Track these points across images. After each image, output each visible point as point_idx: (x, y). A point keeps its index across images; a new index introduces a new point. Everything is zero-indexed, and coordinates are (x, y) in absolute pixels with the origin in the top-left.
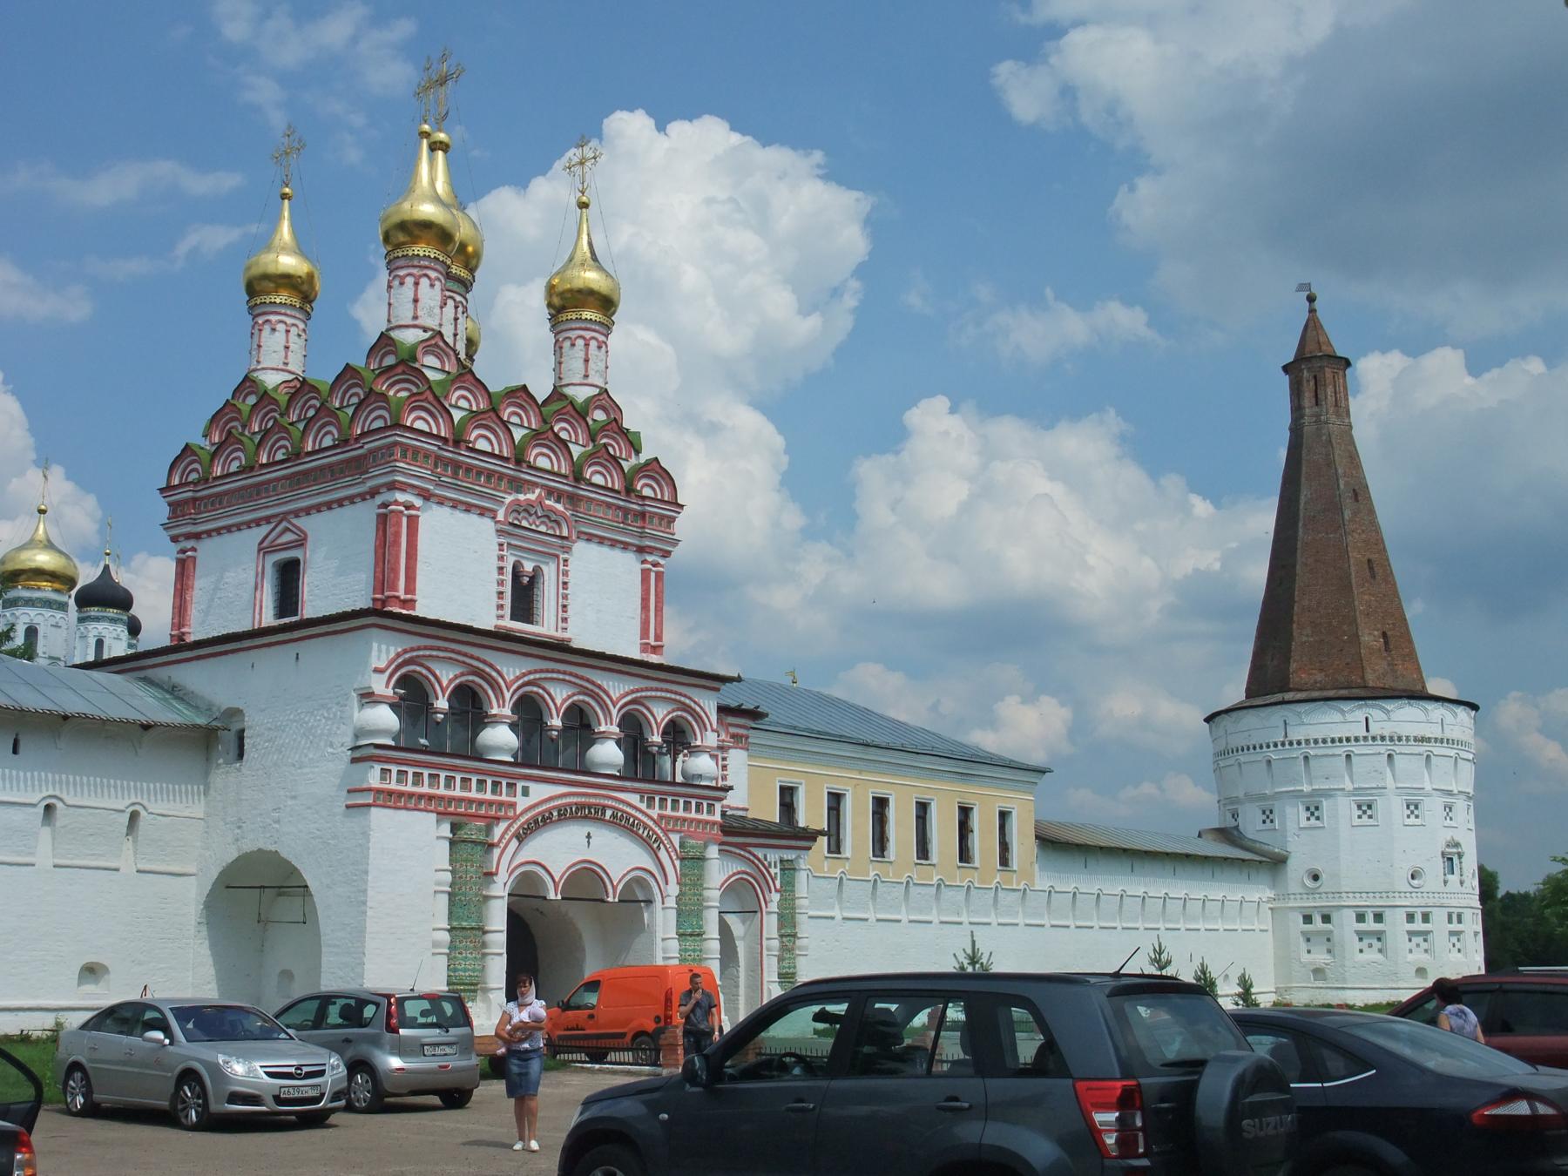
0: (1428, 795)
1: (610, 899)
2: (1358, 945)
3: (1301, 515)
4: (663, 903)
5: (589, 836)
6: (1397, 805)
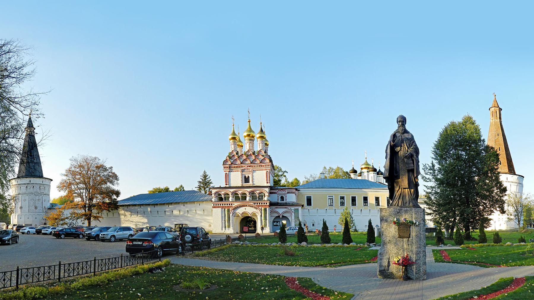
1: (250, 216)
5: (245, 209)
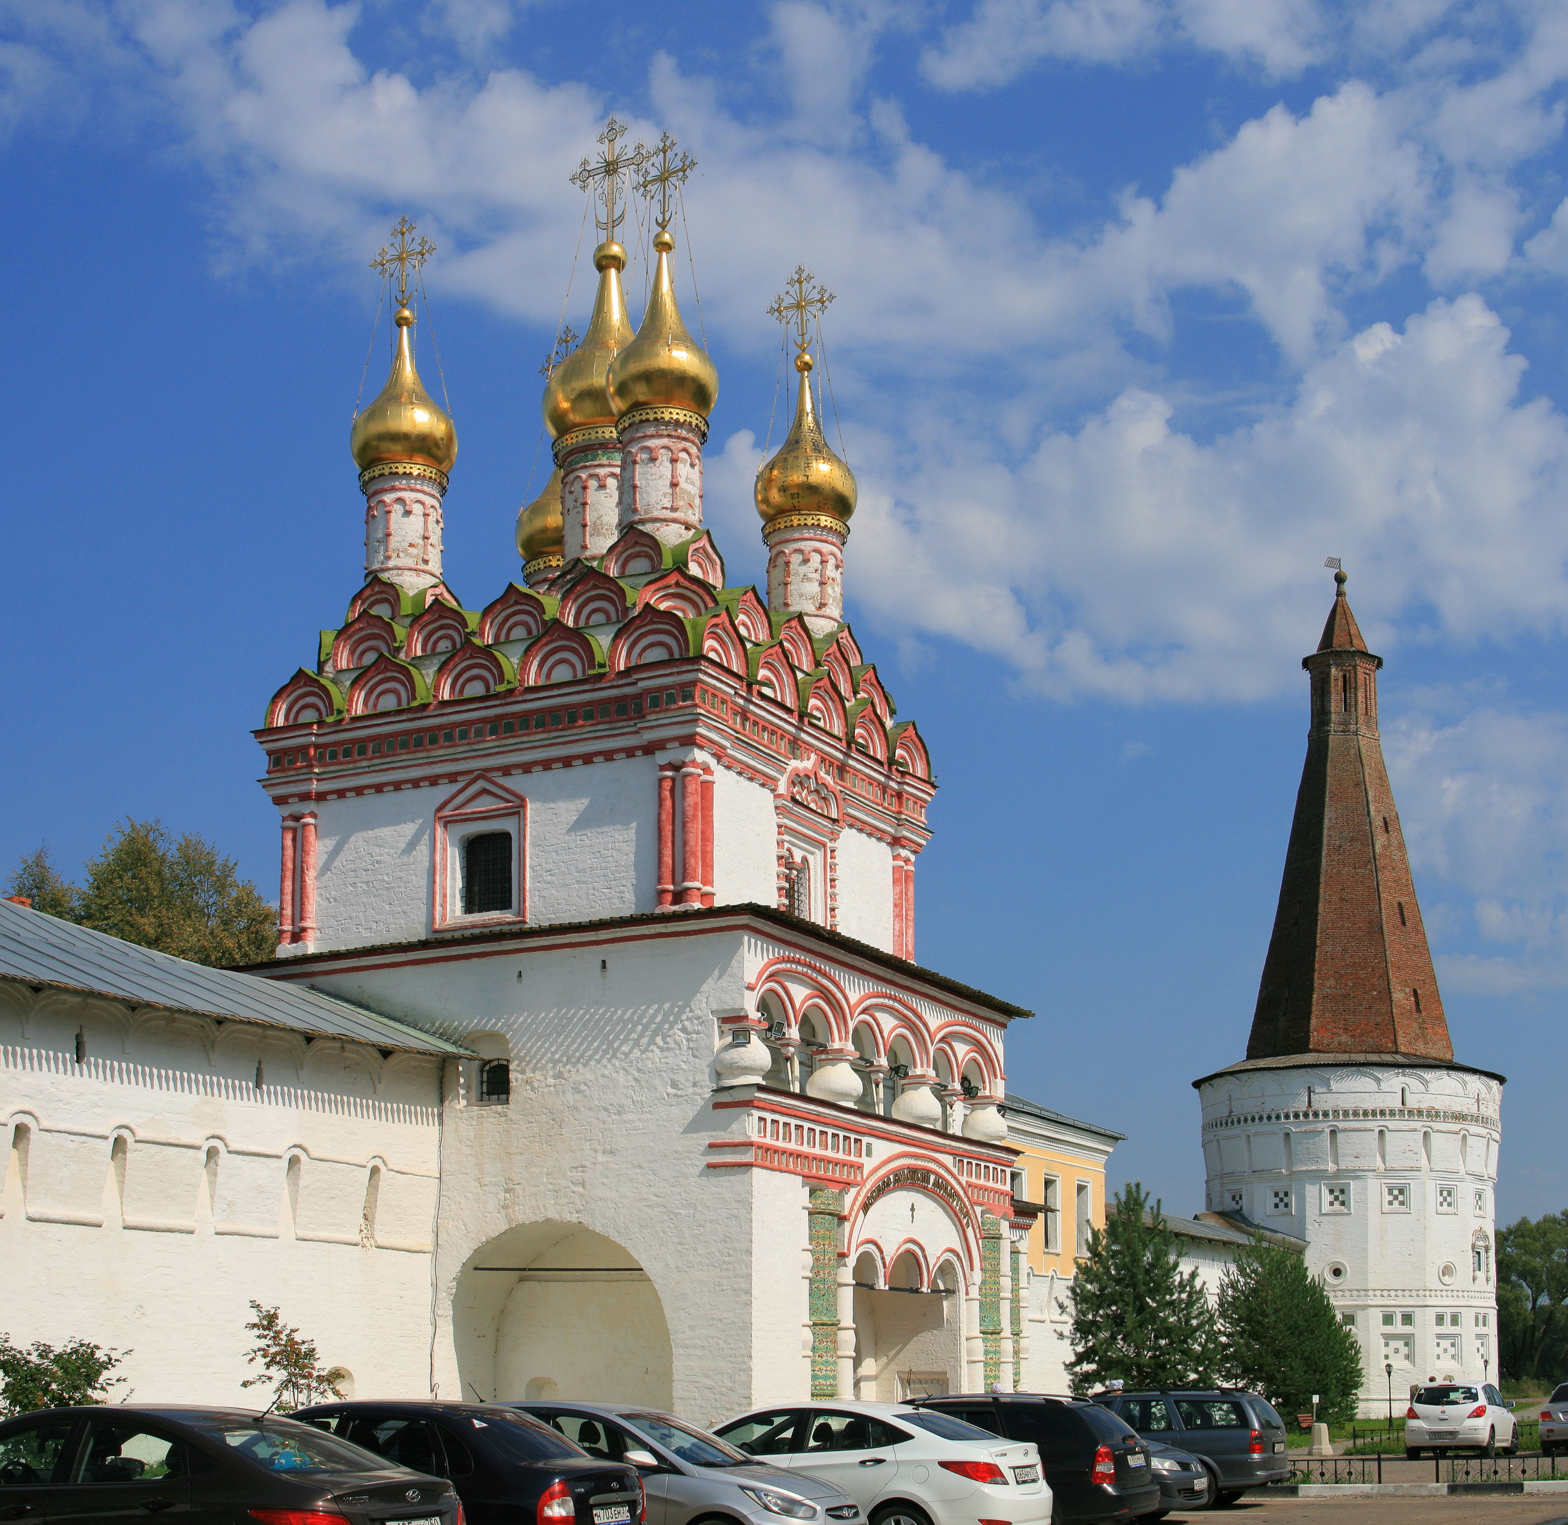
0: (1461, 1180)
2: (1384, 1351)
3: (1325, 842)
4: (967, 1294)
6: (1431, 1190)
